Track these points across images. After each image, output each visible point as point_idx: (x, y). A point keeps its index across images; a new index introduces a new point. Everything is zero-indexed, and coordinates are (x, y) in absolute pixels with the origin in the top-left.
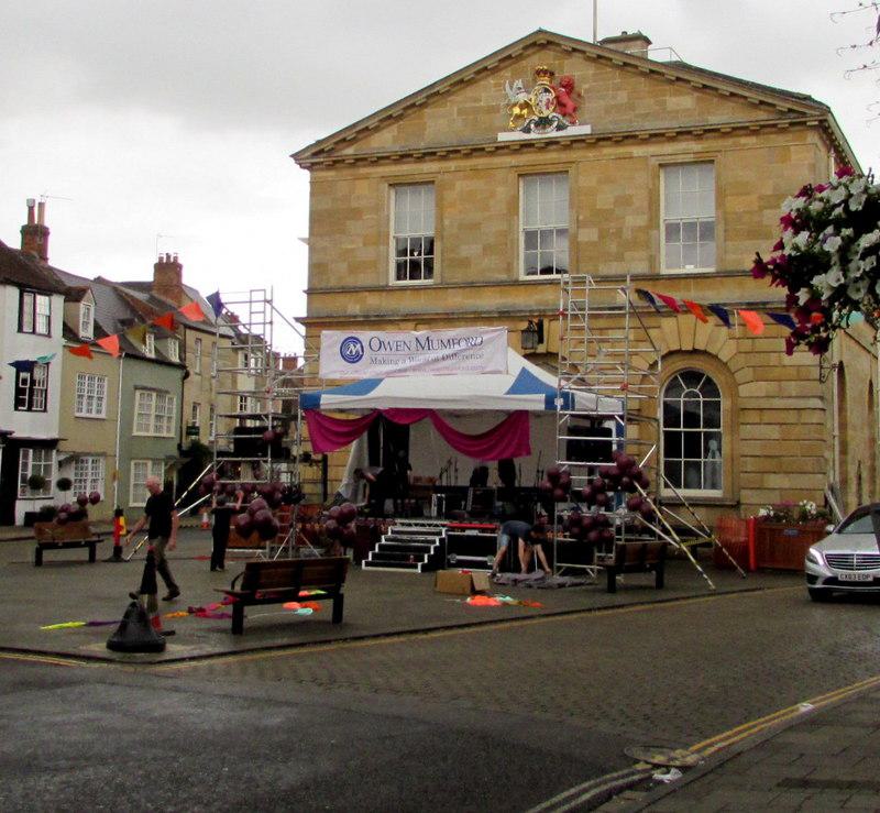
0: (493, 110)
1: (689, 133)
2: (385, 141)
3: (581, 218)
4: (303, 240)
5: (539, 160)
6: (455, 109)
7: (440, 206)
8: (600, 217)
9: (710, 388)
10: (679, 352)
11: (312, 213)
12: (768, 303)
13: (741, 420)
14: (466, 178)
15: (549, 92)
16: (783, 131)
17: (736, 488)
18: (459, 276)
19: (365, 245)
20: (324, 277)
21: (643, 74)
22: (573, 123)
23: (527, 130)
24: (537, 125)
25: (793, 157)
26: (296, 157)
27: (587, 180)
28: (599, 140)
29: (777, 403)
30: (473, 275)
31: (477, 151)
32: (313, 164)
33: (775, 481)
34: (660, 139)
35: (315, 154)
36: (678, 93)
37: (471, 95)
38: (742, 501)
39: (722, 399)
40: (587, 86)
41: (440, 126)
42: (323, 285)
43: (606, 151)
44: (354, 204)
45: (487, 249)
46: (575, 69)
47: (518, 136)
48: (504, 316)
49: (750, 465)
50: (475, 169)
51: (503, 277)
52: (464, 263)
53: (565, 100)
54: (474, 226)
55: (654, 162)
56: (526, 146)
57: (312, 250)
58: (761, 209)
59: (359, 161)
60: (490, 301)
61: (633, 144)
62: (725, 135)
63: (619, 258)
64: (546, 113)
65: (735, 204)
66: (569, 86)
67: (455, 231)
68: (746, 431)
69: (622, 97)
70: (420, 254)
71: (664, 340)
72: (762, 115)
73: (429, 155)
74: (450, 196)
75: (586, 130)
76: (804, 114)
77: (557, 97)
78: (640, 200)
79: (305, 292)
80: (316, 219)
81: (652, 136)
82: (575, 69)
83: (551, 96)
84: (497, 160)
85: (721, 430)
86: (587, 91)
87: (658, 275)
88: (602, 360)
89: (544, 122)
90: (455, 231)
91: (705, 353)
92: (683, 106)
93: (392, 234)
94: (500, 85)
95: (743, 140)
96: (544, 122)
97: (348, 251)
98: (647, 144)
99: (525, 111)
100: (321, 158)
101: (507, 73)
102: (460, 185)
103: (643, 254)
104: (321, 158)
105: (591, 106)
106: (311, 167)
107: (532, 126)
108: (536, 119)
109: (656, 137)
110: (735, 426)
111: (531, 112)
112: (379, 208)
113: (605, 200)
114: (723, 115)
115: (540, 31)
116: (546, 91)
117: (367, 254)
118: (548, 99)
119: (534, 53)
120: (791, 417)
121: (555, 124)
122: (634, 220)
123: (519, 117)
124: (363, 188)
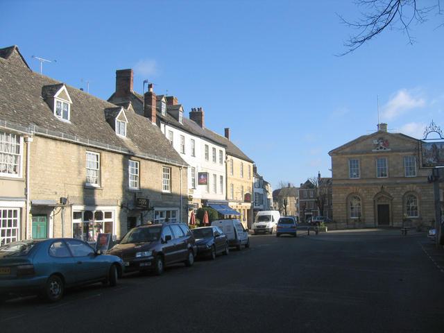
2: (347, 150)
47: (376, 150)
56: (378, 152)
57: (333, 172)
59: (342, 154)
60: (372, 182)
66: (387, 141)
84: (372, 155)
89: (381, 148)
100: (332, 153)
104: (332, 153)
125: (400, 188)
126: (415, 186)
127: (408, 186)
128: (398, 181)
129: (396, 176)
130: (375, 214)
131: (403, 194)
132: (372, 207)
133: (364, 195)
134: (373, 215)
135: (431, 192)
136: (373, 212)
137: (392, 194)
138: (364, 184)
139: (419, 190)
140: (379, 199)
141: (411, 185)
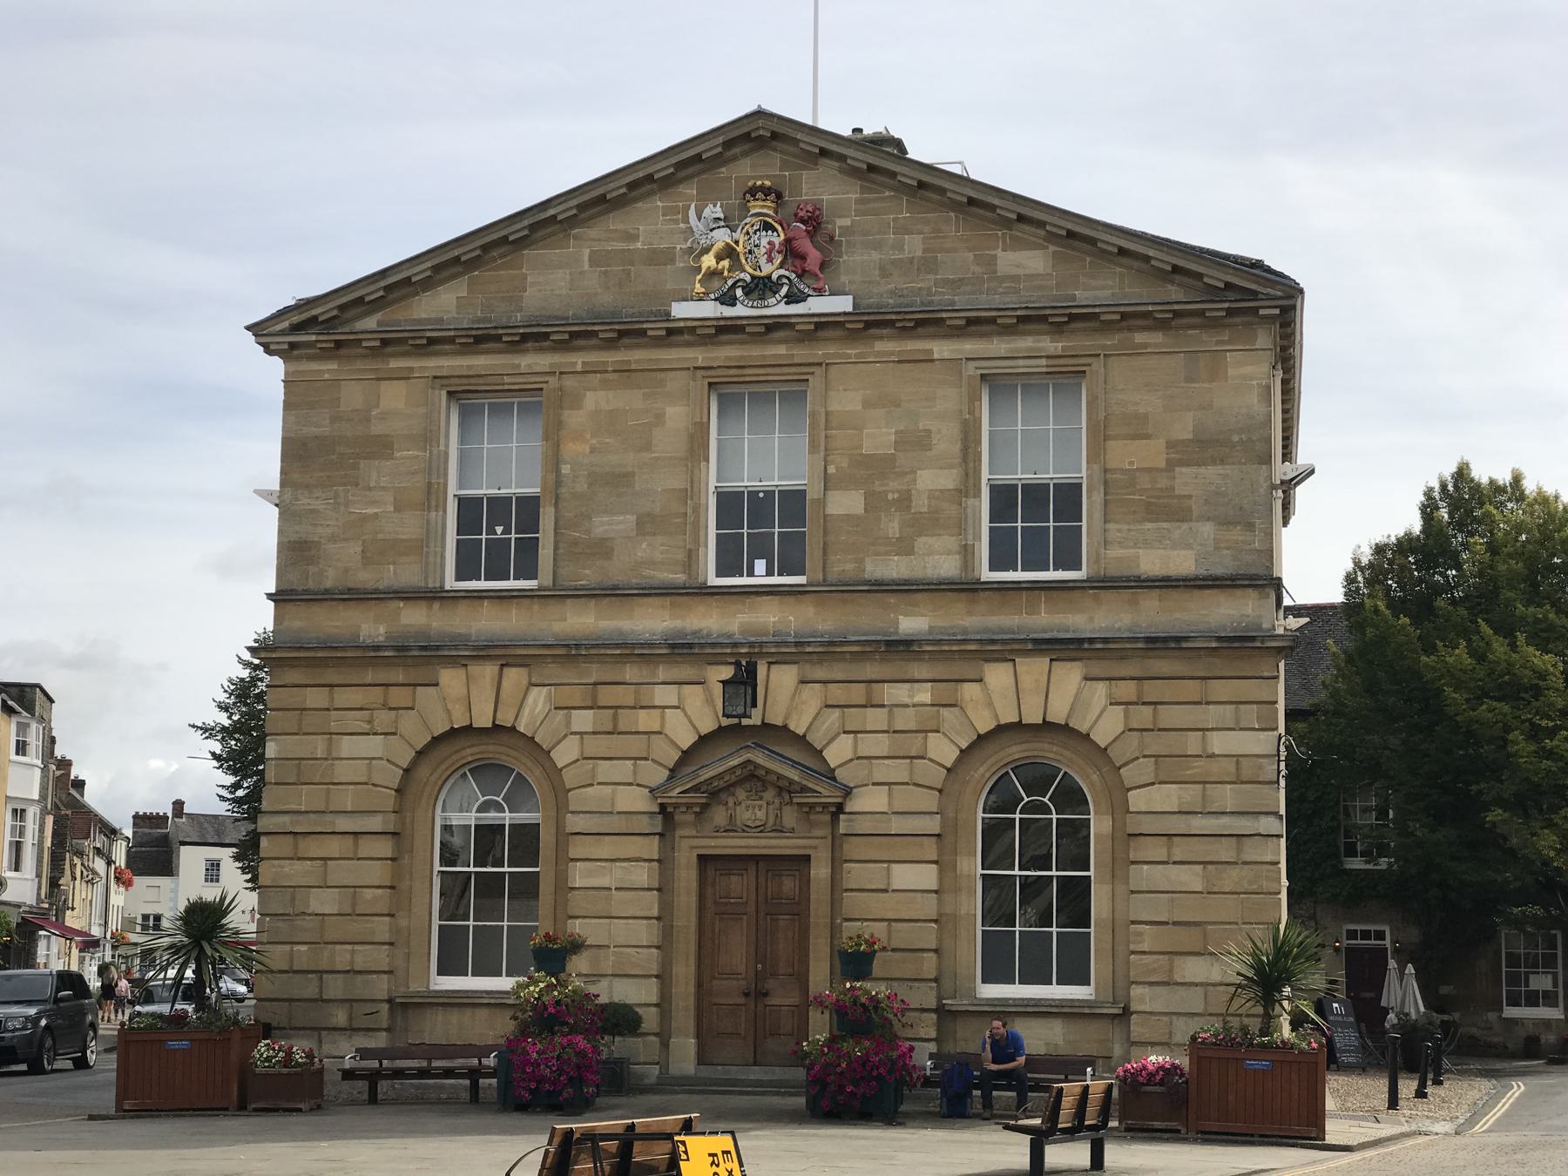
0: (659, 258)
1: (1043, 319)
2: (444, 305)
3: (832, 469)
4: (264, 494)
5: (754, 363)
6: (587, 252)
7: (553, 437)
8: (869, 470)
9: (1071, 797)
10: (1018, 727)
11: (284, 439)
12: (1186, 639)
13: (1132, 857)
14: (606, 385)
15: (774, 230)
16: (1213, 324)
17: (1120, 984)
18: (589, 575)
19: (397, 509)
20: (312, 569)
21: (955, 206)
22: (820, 292)
23: (728, 299)
24: (748, 291)
25: (1231, 372)
26: (256, 329)
27: (845, 401)
28: (868, 325)
29: (1199, 824)
30: (617, 570)
31: (628, 334)
32: (293, 346)
33: (1194, 969)
34: (985, 328)
35: (297, 328)
36: (1016, 244)
37: (620, 227)
38: (1134, 1007)
39: (1092, 817)
40: (846, 222)
41: (553, 283)
42: (311, 585)
43: (880, 346)
44: (377, 429)
45: (647, 524)
46: (822, 188)
47: (710, 309)
48: (682, 649)
49: (1148, 939)
50: (624, 370)
51: (680, 578)
52: (602, 549)
53: (805, 245)
54: (620, 480)
55: (971, 369)
56: (726, 330)
58: (1171, 465)
59: (388, 344)
60: (651, 621)
61: (934, 337)
62: (1108, 327)
63: (904, 547)
64: (767, 269)
65: (1124, 455)
67: (581, 486)
68: (1143, 876)
69: (914, 245)
70: (507, 531)
71: (990, 704)
72: (1174, 293)
73: (532, 337)
74: (574, 419)
75: (843, 304)
76: (1255, 293)
77: (788, 241)
78: (946, 440)
79: (269, 596)
80: (295, 452)
81: (971, 322)
82: (822, 188)
83: (778, 239)
85: (1091, 873)
86: (846, 231)
87: (978, 582)
88: (876, 745)
89: (761, 287)
90: (581, 486)
91: (1065, 729)
92: (1027, 265)
93: (452, 489)
94: (675, 211)
95: (1140, 338)
96: (761, 287)
97: (364, 518)
98: (1012, 334)
99: (726, 263)
101: (690, 190)
102: (596, 400)
103: (951, 542)
104: (310, 334)
105: (856, 261)
106: (288, 353)
107: (739, 292)
108: (748, 279)
109: (976, 325)
110: (1120, 865)
111: (736, 265)
112: (429, 437)
113: (879, 438)
114: (1101, 288)
115: (759, 114)
116: (767, 227)
117: (408, 527)
118: (770, 243)
119: (745, 154)
120: (1225, 851)
121: (784, 290)
122: (933, 480)
123: (713, 274)
124: (394, 396)
125: (924, 695)
126: (1069, 677)
127: (998, 676)
128: (911, 623)
129: (894, 568)
130: (664, 946)
131: (944, 751)
132: (642, 875)
133: (564, 754)
134: (650, 960)
135: (1220, 743)
136: (645, 932)
137: (837, 753)
138: (573, 652)
139: (1106, 727)
140: (715, 793)
141: (1033, 668)
